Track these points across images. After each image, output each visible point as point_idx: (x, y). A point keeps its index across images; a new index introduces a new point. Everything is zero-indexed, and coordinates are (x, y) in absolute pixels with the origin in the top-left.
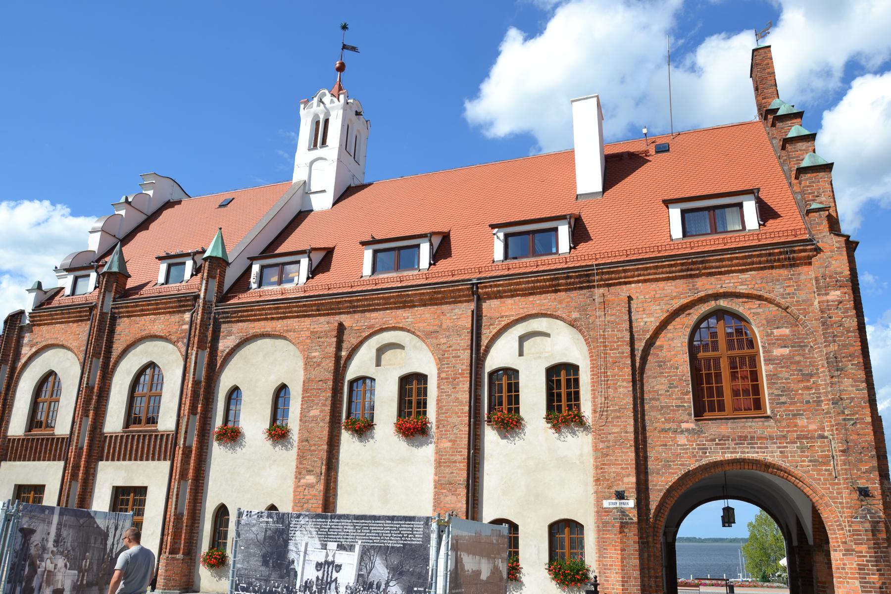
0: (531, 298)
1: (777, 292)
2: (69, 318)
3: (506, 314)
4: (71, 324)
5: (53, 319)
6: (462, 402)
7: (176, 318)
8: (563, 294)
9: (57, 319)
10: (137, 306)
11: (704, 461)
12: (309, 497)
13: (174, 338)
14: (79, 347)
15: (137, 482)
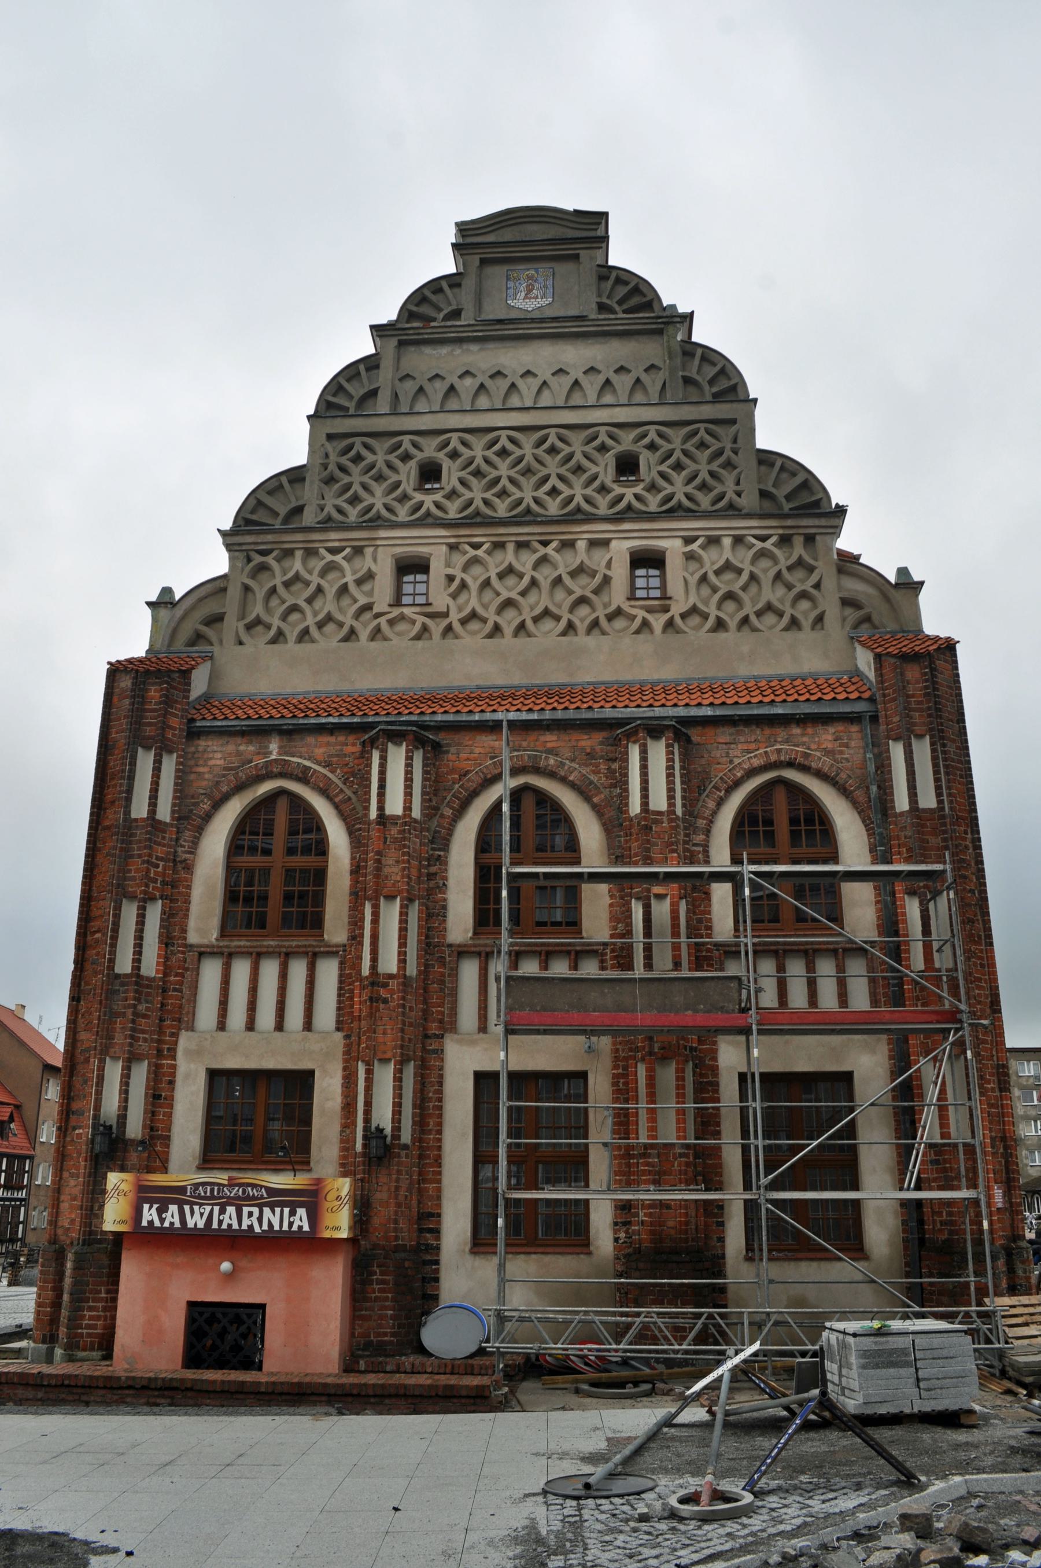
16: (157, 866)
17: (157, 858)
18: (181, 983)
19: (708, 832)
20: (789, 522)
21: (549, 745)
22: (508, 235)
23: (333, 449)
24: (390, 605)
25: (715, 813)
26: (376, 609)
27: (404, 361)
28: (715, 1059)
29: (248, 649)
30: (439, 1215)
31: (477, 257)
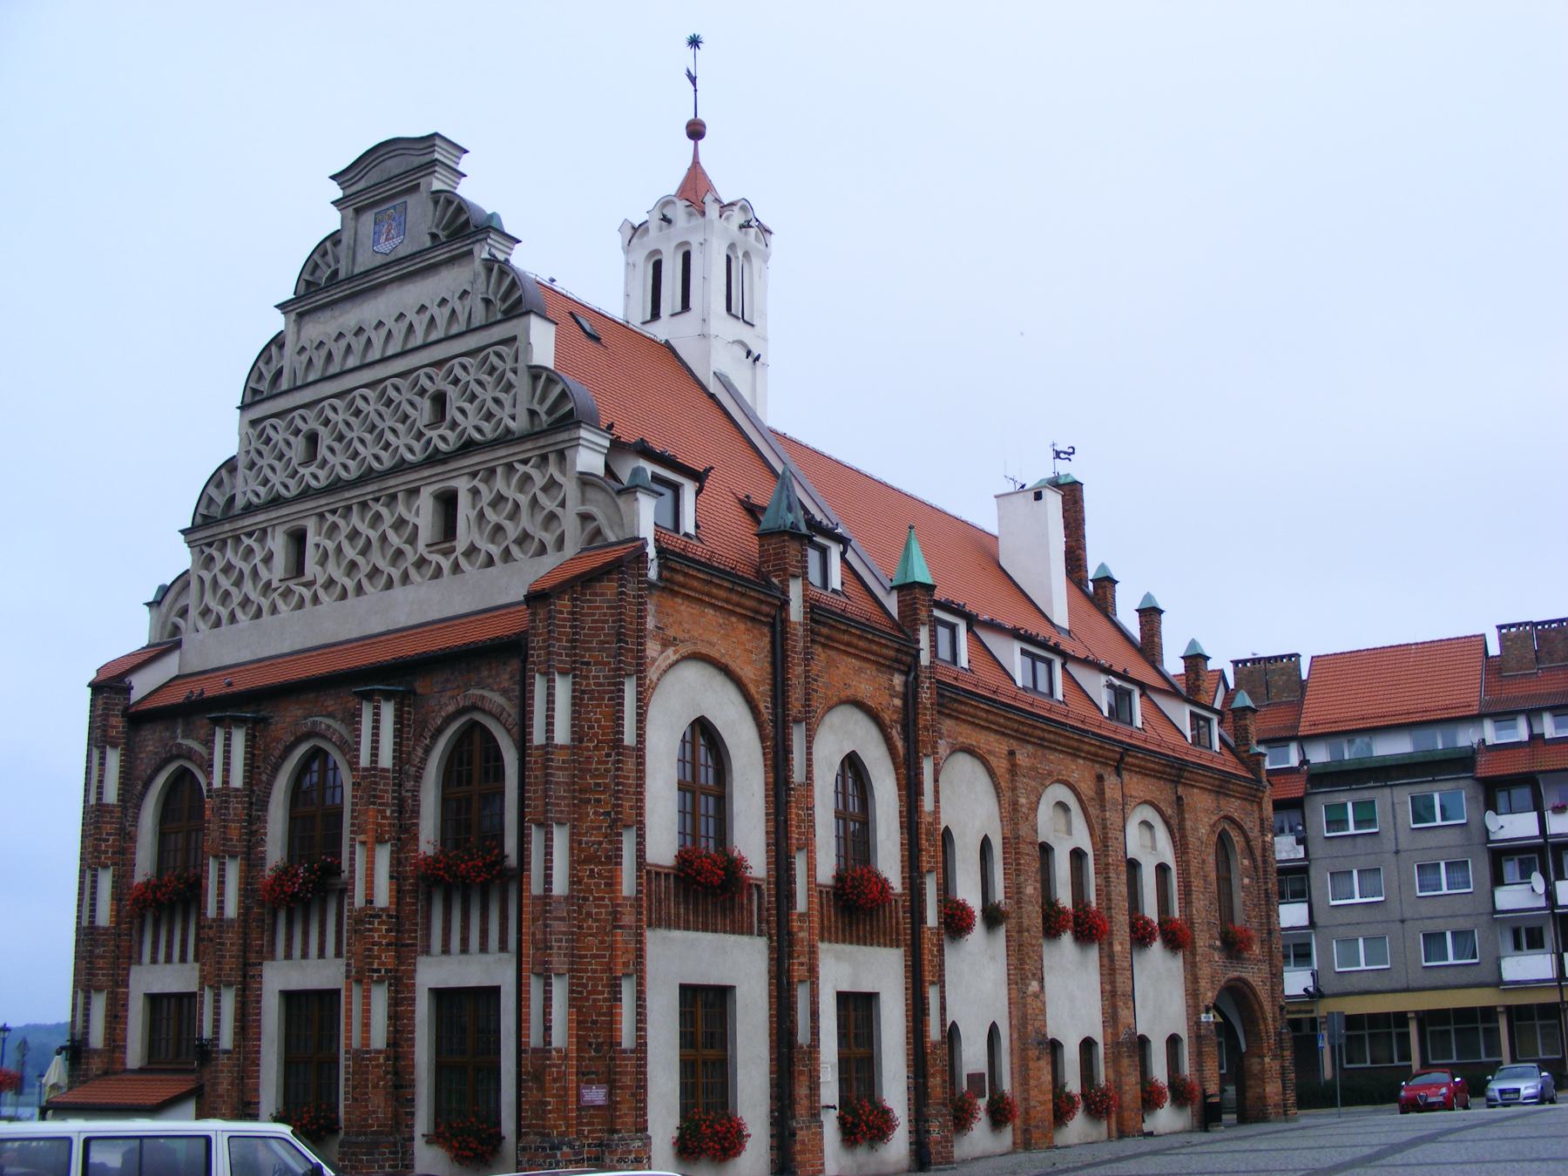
0: (1147, 780)
1: (1247, 825)
2: (738, 605)
3: (1134, 794)
4: (734, 619)
5: (708, 595)
6: (1122, 896)
7: (883, 679)
8: (1162, 782)
9: (716, 598)
10: (845, 632)
11: (1226, 979)
12: (1037, 1011)
13: (887, 717)
14: (757, 683)
15: (865, 987)
16: (108, 840)
17: (107, 834)
18: (131, 929)
19: (418, 778)
20: (542, 442)
21: (330, 709)
22: (373, 177)
23: (253, 433)
24: (280, 581)
25: (424, 760)
26: (273, 586)
27: (303, 334)
28: (413, 978)
29: (200, 636)
30: (258, 1103)
31: (351, 209)
